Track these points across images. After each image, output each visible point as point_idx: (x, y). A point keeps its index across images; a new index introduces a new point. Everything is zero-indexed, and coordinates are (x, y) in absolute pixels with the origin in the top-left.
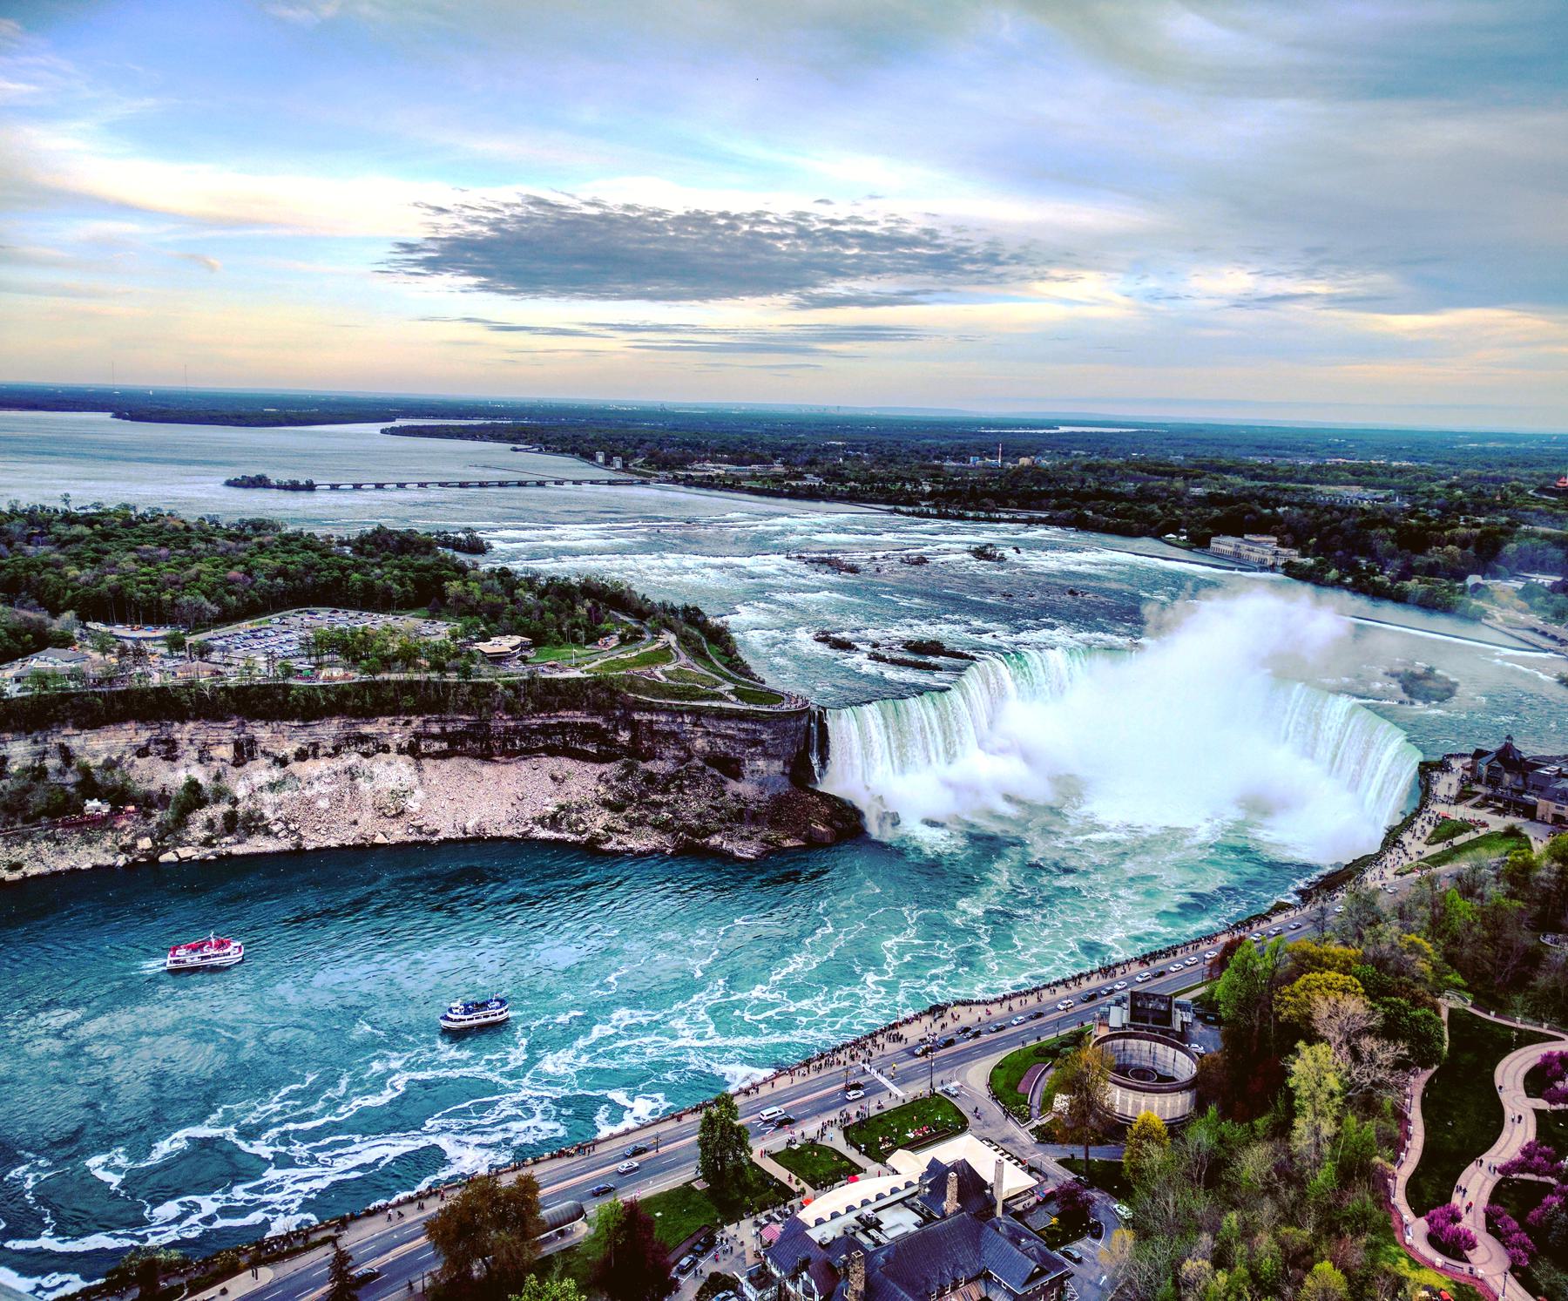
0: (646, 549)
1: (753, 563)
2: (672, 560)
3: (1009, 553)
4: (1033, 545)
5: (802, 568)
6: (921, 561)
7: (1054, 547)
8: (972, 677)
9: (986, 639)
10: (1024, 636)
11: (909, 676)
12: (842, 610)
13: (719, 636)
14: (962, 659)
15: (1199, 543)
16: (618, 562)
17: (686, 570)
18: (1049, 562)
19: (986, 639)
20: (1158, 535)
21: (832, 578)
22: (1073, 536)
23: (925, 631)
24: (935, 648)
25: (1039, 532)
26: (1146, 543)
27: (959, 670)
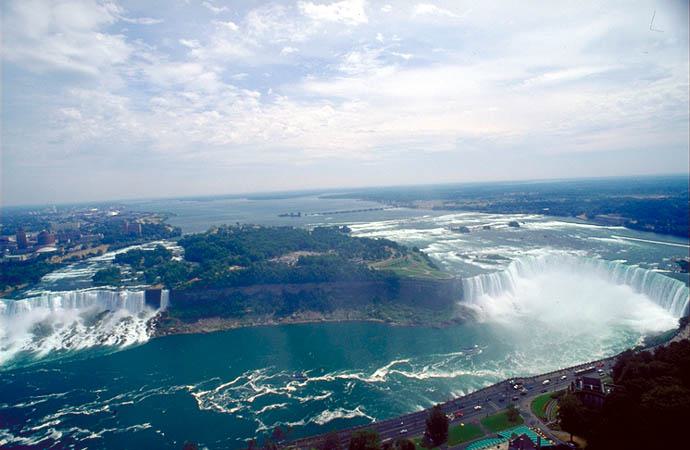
0: (398, 228)
1: (435, 231)
2: (407, 231)
3: (521, 224)
4: (530, 221)
5: (450, 232)
6: (488, 228)
7: (536, 221)
8: (512, 266)
9: (515, 253)
10: (528, 252)
11: (490, 267)
12: (466, 245)
13: (425, 255)
14: (507, 260)
15: (591, 219)
16: (390, 233)
17: (411, 234)
18: (537, 226)
19: (515, 253)
20: (574, 216)
21: (460, 235)
22: (543, 217)
23: (493, 251)
24: (496, 257)
25: (530, 217)
26: (570, 218)
27: (507, 264)
